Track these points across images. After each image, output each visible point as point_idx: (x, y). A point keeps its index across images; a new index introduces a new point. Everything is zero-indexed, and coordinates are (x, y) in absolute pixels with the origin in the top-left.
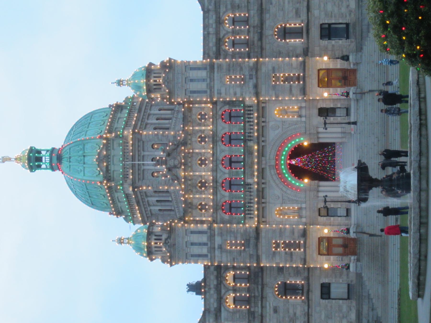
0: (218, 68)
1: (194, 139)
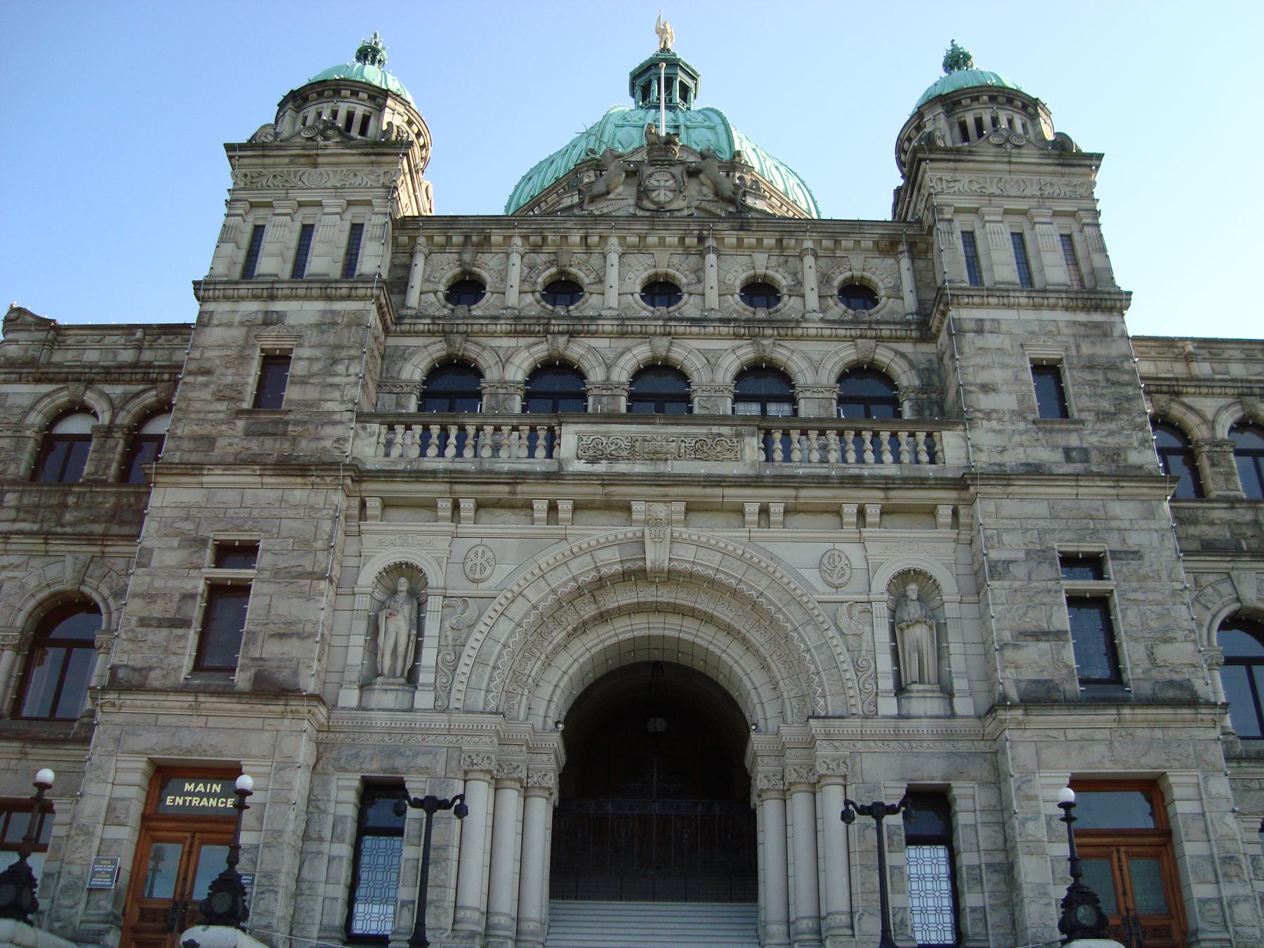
0: (1097, 325)
1: (760, 259)
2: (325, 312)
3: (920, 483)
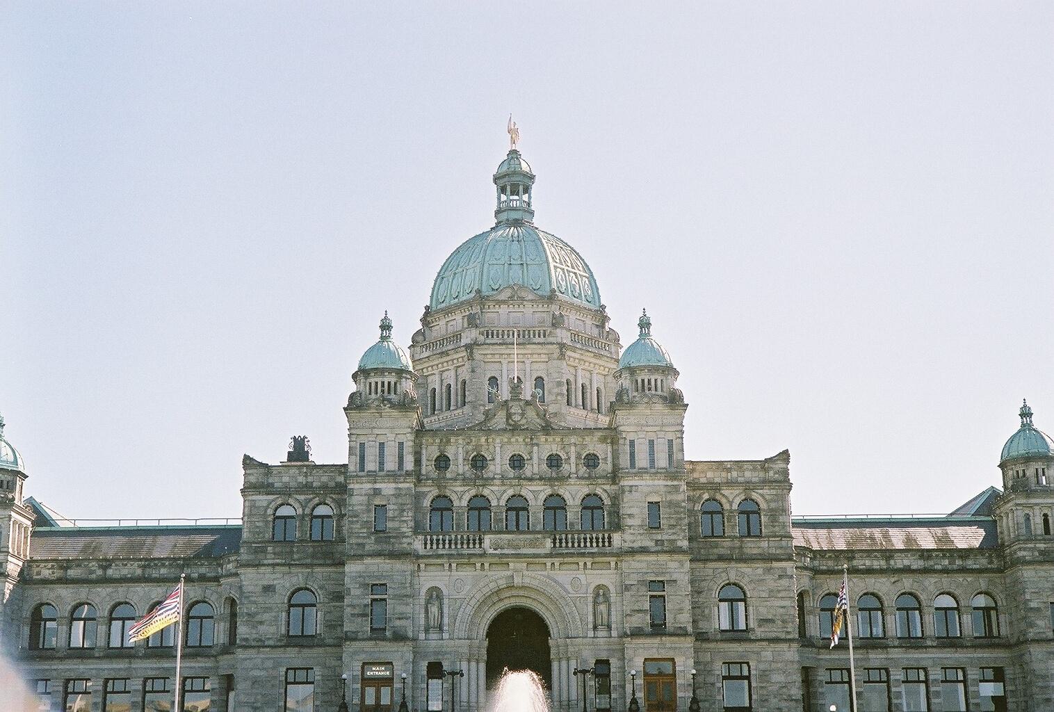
2: (396, 489)
3: (605, 555)
